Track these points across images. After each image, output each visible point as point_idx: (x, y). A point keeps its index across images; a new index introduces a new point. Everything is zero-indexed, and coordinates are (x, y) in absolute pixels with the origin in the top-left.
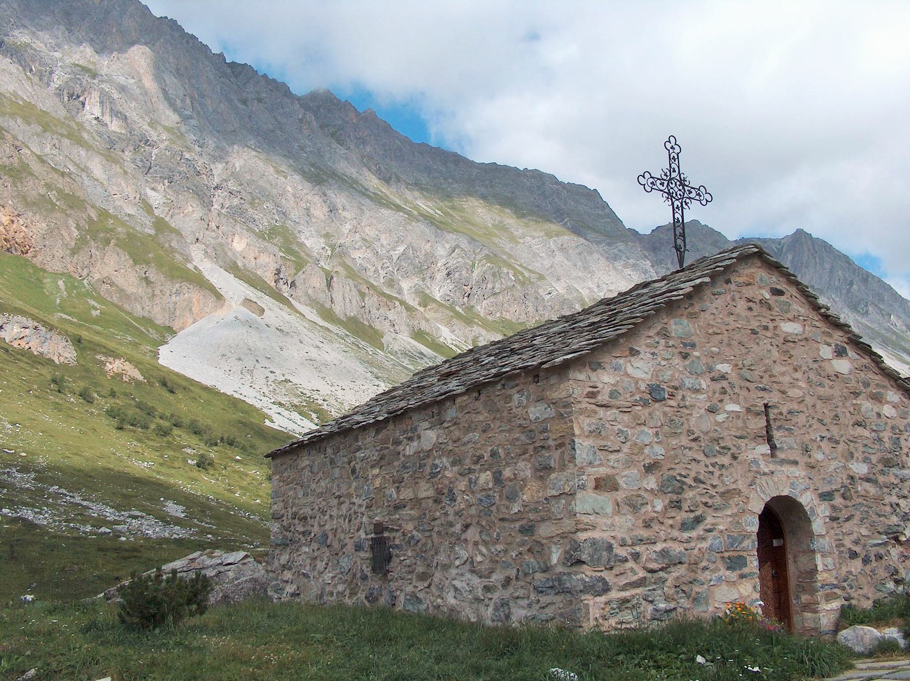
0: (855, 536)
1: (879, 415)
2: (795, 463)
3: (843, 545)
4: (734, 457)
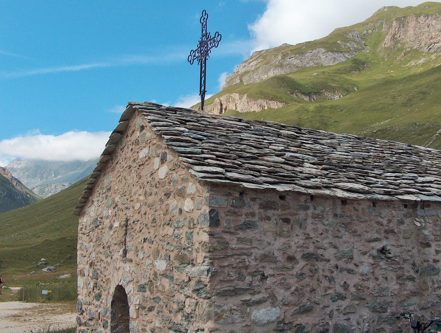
1: (181, 211)
2: (131, 261)
4: (112, 258)
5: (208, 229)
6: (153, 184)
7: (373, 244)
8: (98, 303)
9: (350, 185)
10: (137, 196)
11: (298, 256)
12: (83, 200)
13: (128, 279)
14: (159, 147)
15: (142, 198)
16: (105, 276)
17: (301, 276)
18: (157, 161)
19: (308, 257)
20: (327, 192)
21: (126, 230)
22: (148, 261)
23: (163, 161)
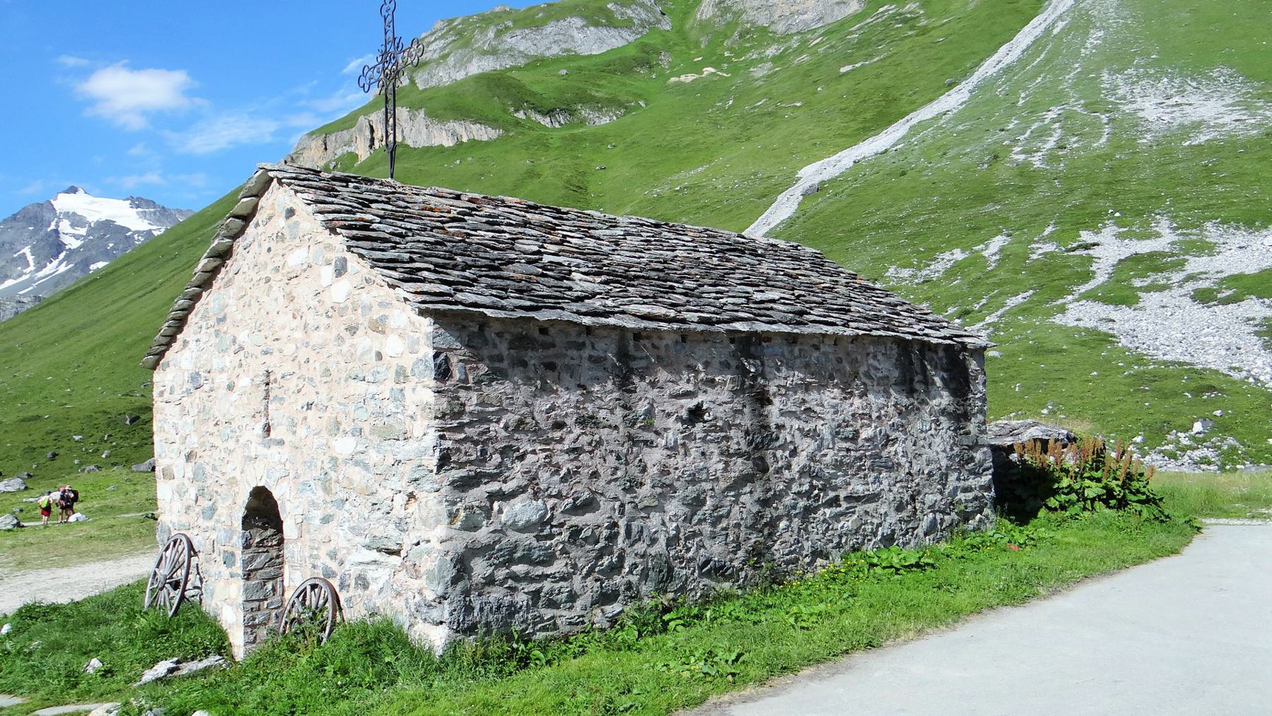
0: (332, 546)
1: (379, 356)
2: (281, 443)
3: (317, 557)
5: (433, 383)
6: (322, 310)
7: (683, 401)
8: (210, 524)
9: (645, 309)
10: (287, 332)
11: (569, 421)
12: (164, 340)
13: (278, 475)
14: (329, 247)
15: (299, 335)
16: (223, 474)
17: (575, 451)
18: (329, 271)
19: (582, 422)
20: (611, 321)
21: (267, 391)
22: (317, 441)
23: (341, 270)
